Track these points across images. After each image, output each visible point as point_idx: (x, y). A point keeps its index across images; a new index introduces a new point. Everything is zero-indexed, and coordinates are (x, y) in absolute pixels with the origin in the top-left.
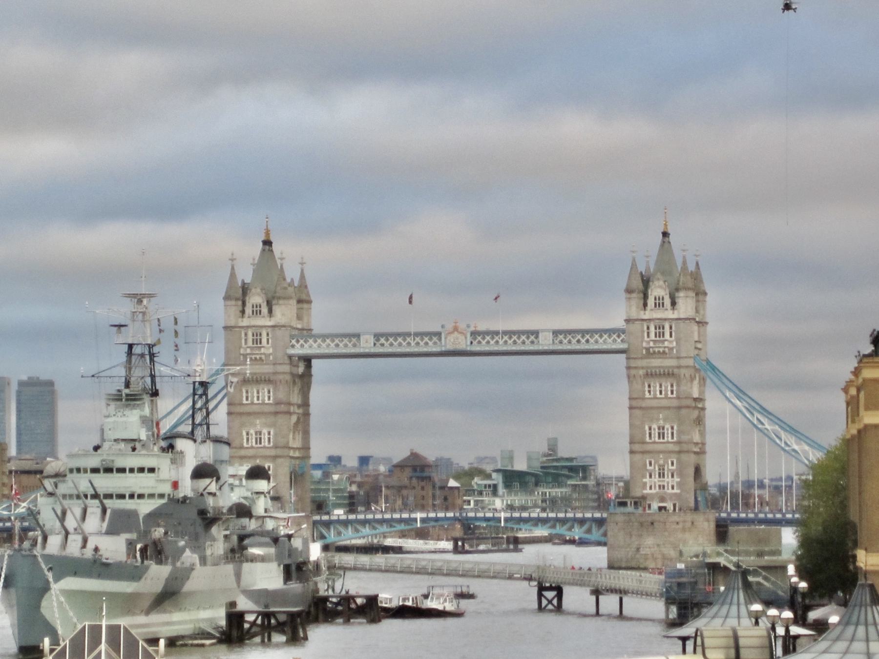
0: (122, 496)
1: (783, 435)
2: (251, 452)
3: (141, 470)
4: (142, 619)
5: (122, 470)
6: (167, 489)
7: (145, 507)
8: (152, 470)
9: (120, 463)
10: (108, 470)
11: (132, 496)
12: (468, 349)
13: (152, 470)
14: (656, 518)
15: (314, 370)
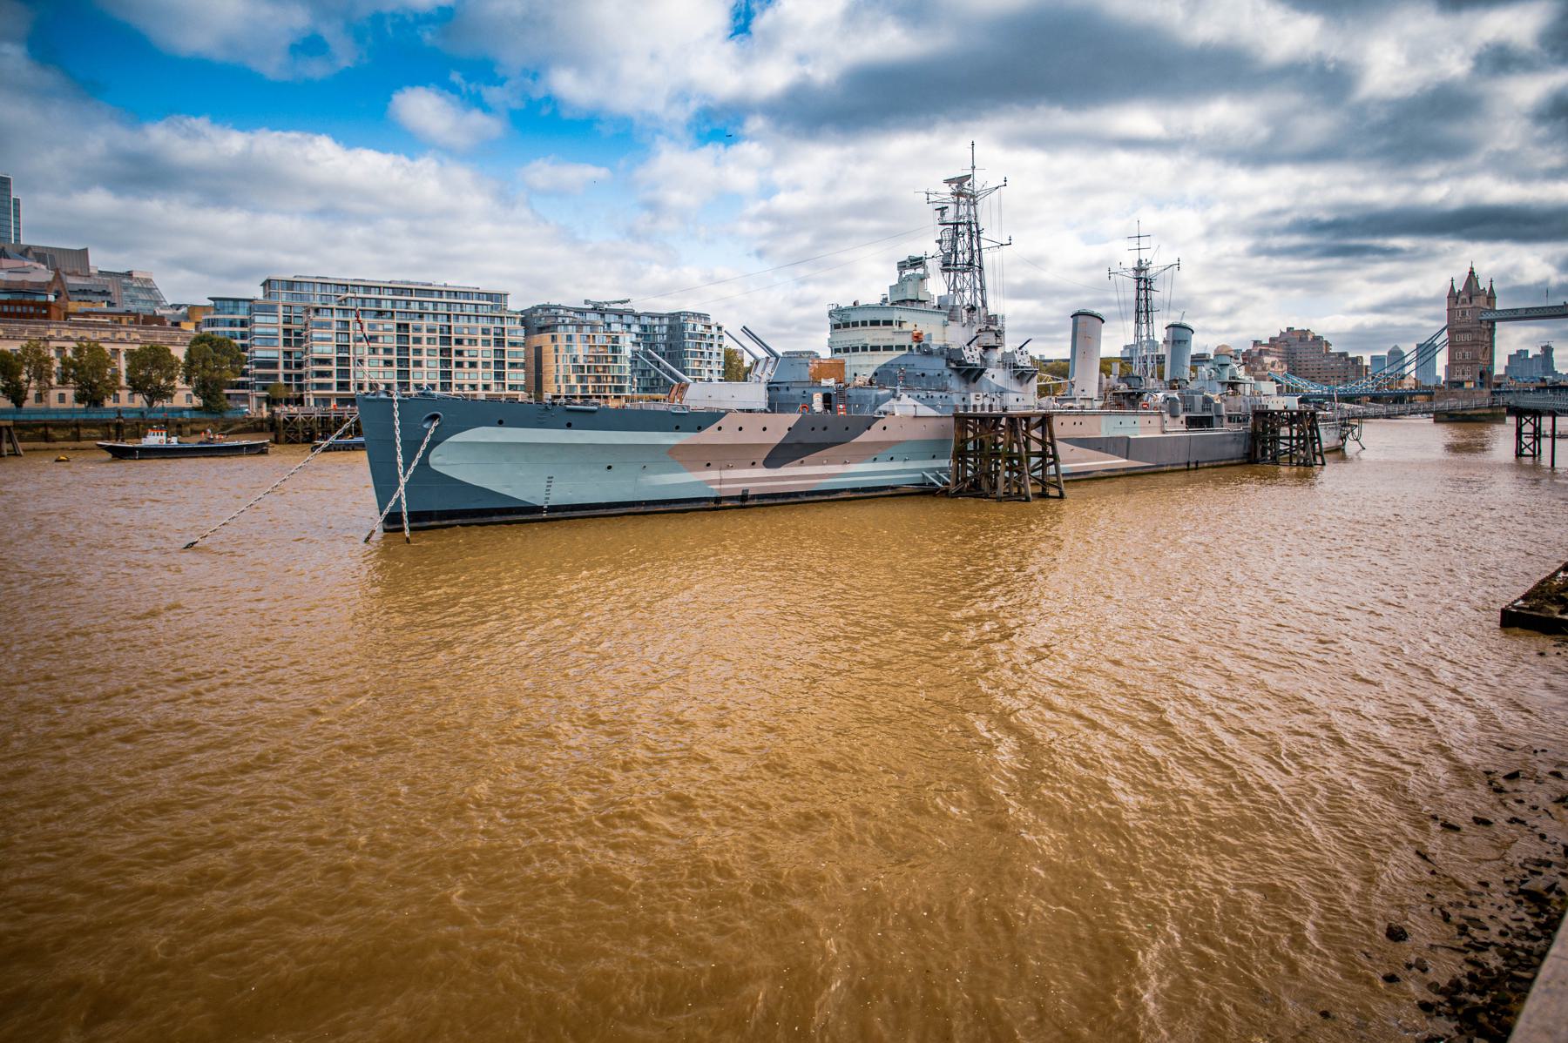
0: (855, 349)
3: (875, 323)
5: (855, 324)
6: (907, 340)
9: (855, 317)
10: (846, 325)
11: (864, 349)
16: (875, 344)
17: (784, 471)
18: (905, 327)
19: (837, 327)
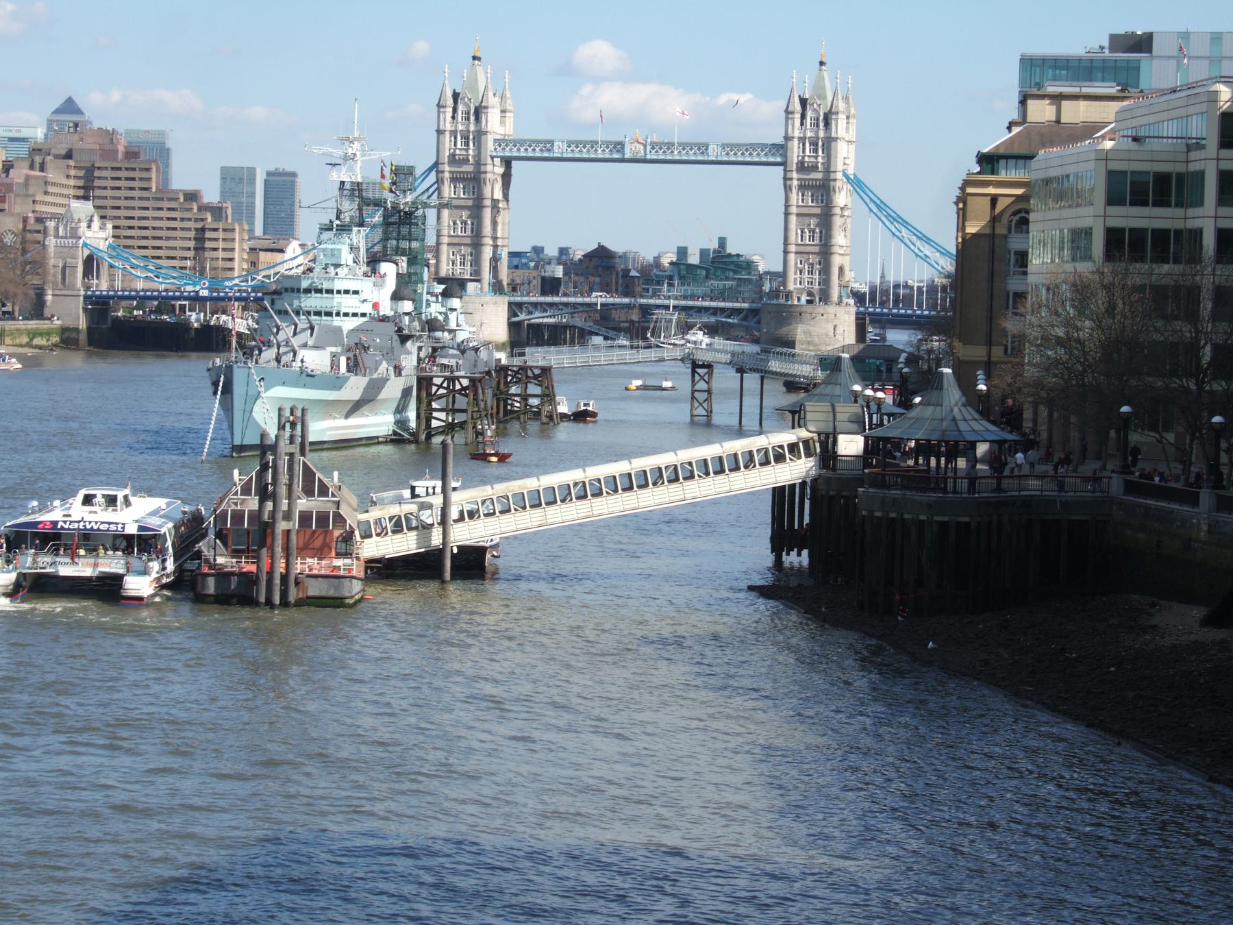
0: (329, 314)
1: (918, 243)
2: (456, 240)
3: (347, 292)
4: (342, 422)
5: (329, 291)
6: (367, 308)
7: (348, 324)
8: (356, 292)
10: (319, 291)
11: (338, 314)
12: (648, 157)
13: (356, 292)
14: (804, 309)
15: (513, 171)
16: (346, 311)
17: (353, 421)
18: (363, 296)
19: (308, 291)
